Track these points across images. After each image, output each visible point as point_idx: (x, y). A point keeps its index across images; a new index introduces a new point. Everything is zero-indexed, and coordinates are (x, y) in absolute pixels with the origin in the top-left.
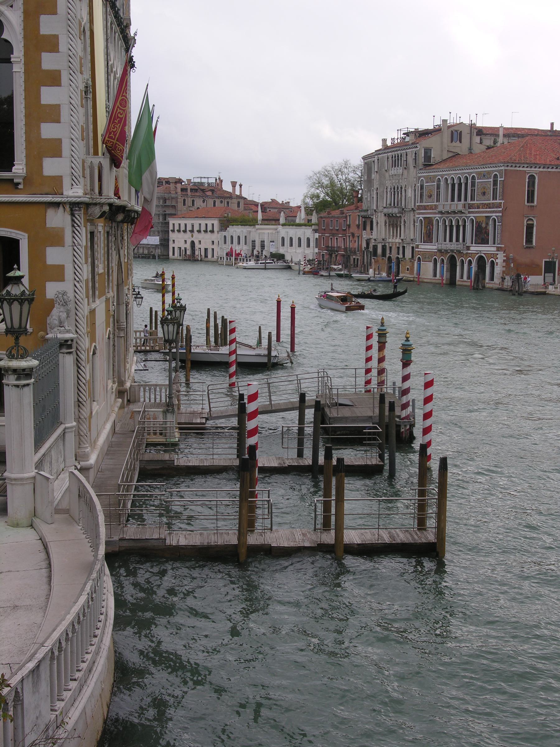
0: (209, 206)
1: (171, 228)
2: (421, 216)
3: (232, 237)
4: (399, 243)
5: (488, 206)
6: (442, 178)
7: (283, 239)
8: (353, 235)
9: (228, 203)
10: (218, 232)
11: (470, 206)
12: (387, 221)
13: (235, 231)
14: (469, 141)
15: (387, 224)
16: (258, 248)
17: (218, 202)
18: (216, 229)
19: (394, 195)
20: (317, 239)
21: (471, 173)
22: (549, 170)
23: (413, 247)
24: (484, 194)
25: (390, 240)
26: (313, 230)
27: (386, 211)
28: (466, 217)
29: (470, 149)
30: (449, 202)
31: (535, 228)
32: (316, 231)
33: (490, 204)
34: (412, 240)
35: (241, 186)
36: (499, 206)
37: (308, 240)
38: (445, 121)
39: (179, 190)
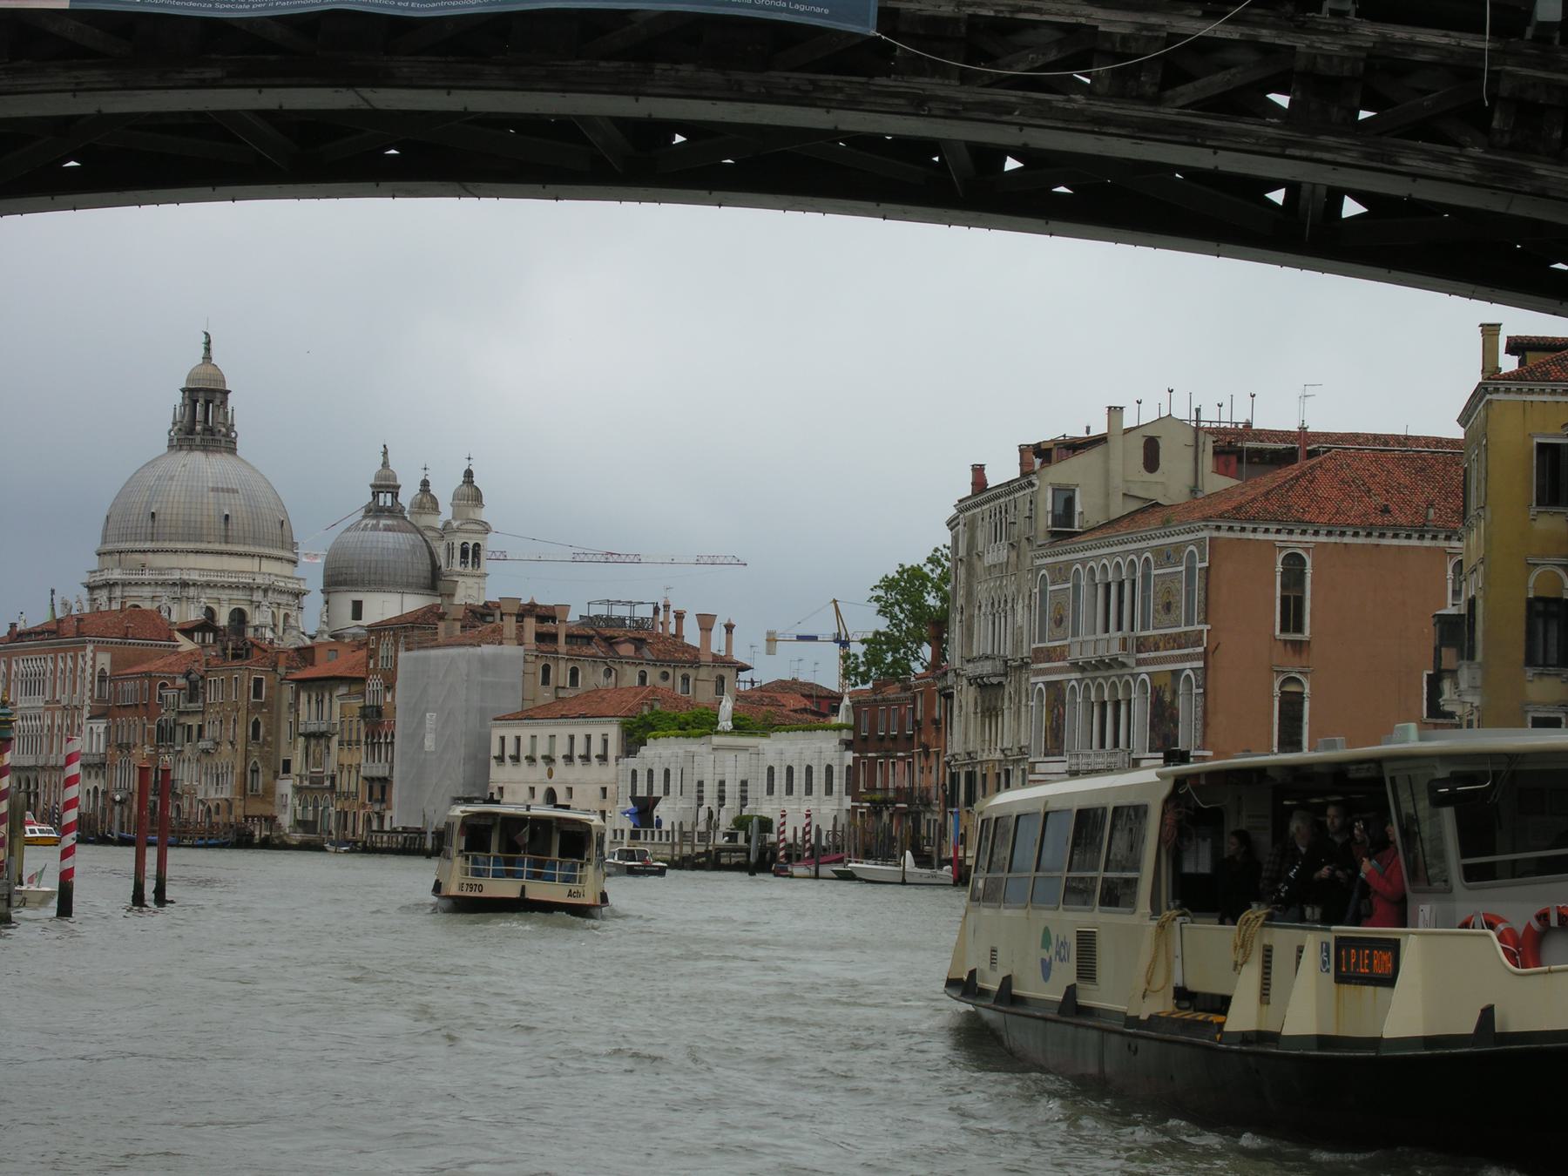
0: (625, 683)
1: (495, 751)
2: (1041, 679)
3: (650, 772)
4: (1000, 761)
5: (1177, 641)
6: (1084, 567)
7: (771, 770)
8: (926, 748)
9: (686, 679)
10: (617, 759)
11: (1142, 645)
12: (979, 701)
13: (660, 752)
14: (1188, 466)
15: (978, 710)
16: (710, 800)
17: (653, 675)
18: (613, 751)
19: (994, 623)
20: (849, 767)
21: (1143, 550)
22: (1347, 540)
23: (1024, 770)
24: (1168, 607)
25: (985, 758)
26: (842, 742)
27: (971, 669)
28: (1132, 675)
29: (1194, 490)
30: (1100, 635)
31: (1307, 705)
32: (848, 745)
33: (1179, 635)
34: (1020, 749)
35: (729, 628)
36: (1195, 639)
37: (829, 769)
38: (1115, 412)
39: (529, 635)
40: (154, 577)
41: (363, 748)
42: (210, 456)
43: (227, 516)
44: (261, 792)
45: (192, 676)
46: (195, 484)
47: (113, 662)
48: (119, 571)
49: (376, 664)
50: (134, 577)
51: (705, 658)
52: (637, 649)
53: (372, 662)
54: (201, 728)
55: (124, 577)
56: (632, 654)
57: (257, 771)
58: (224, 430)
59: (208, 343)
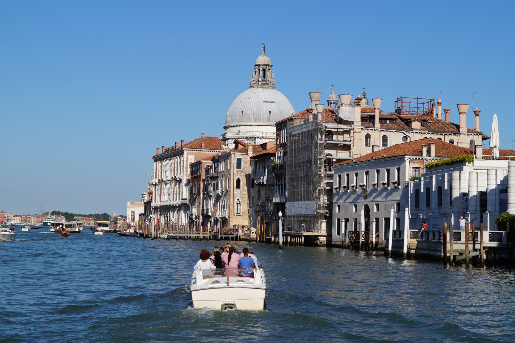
35: (476, 113)
40: (243, 135)
41: (275, 187)
42: (264, 89)
43: (270, 111)
44: (241, 214)
45: (214, 160)
46: (258, 100)
47: (195, 159)
48: (231, 134)
49: (280, 142)
50: (235, 136)
51: (463, 130)
52: (422, 125)
53: (278, 141)
54: (217, 184)
55: (233, 136)
56: (419, 128)
57: (240, 203)
58: (270, 80)
59: (264, 48)
